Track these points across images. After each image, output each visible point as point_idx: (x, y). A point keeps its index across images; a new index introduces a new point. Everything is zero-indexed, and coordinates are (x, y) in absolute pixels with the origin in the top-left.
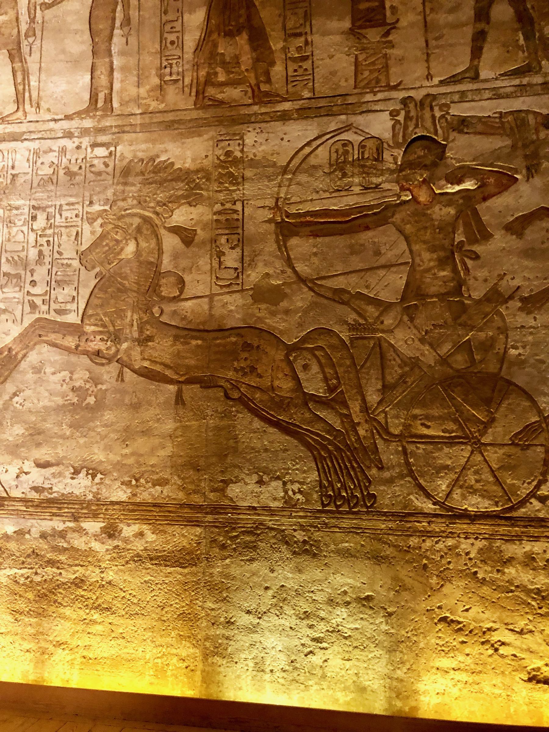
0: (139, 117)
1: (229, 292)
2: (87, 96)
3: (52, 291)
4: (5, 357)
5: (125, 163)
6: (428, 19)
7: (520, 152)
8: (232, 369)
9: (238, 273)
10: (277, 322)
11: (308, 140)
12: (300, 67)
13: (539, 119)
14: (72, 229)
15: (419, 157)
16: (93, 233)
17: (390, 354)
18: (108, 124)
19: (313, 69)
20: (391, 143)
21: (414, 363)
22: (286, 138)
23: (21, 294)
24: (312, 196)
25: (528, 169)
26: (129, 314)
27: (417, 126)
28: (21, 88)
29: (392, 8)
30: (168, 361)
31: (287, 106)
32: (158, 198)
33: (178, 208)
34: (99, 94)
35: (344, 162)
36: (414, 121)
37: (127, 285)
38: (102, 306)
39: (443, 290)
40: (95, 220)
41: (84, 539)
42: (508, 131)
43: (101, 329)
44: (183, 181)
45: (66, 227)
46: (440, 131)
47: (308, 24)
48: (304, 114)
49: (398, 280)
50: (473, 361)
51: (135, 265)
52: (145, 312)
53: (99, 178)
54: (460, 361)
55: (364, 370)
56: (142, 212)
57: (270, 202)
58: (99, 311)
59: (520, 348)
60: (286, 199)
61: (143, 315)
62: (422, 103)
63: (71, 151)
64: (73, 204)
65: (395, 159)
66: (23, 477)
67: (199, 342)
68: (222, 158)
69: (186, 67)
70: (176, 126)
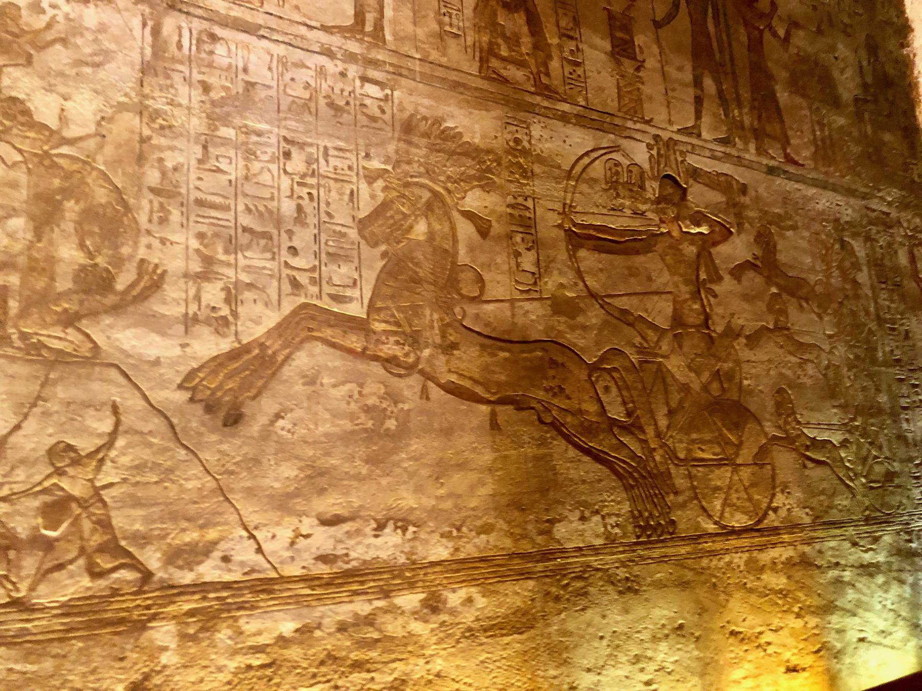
0: (417, 62)
1: (528, 300)
3: (323, 268)
4: (255, 357)
5: (406, 115)
14: (345, 185)
16: (373, 197)
18: (380, 57)
23: (276, 263)
26: (428, 312)
30: (477, 376)
31: (566, 107)
37: (422, 275)
38: (392, 297)
41: (400, 621)
43: (394, 328)
44: (473, 159)
45: (336, 180)
53: (374, 125)
56: (431, 184)
57: (558, 206)
58: (390, 303)
61: (444, 316)
64: (341, 150)
66: (302, 543)
67: (507, 355)
70: (462, 89)
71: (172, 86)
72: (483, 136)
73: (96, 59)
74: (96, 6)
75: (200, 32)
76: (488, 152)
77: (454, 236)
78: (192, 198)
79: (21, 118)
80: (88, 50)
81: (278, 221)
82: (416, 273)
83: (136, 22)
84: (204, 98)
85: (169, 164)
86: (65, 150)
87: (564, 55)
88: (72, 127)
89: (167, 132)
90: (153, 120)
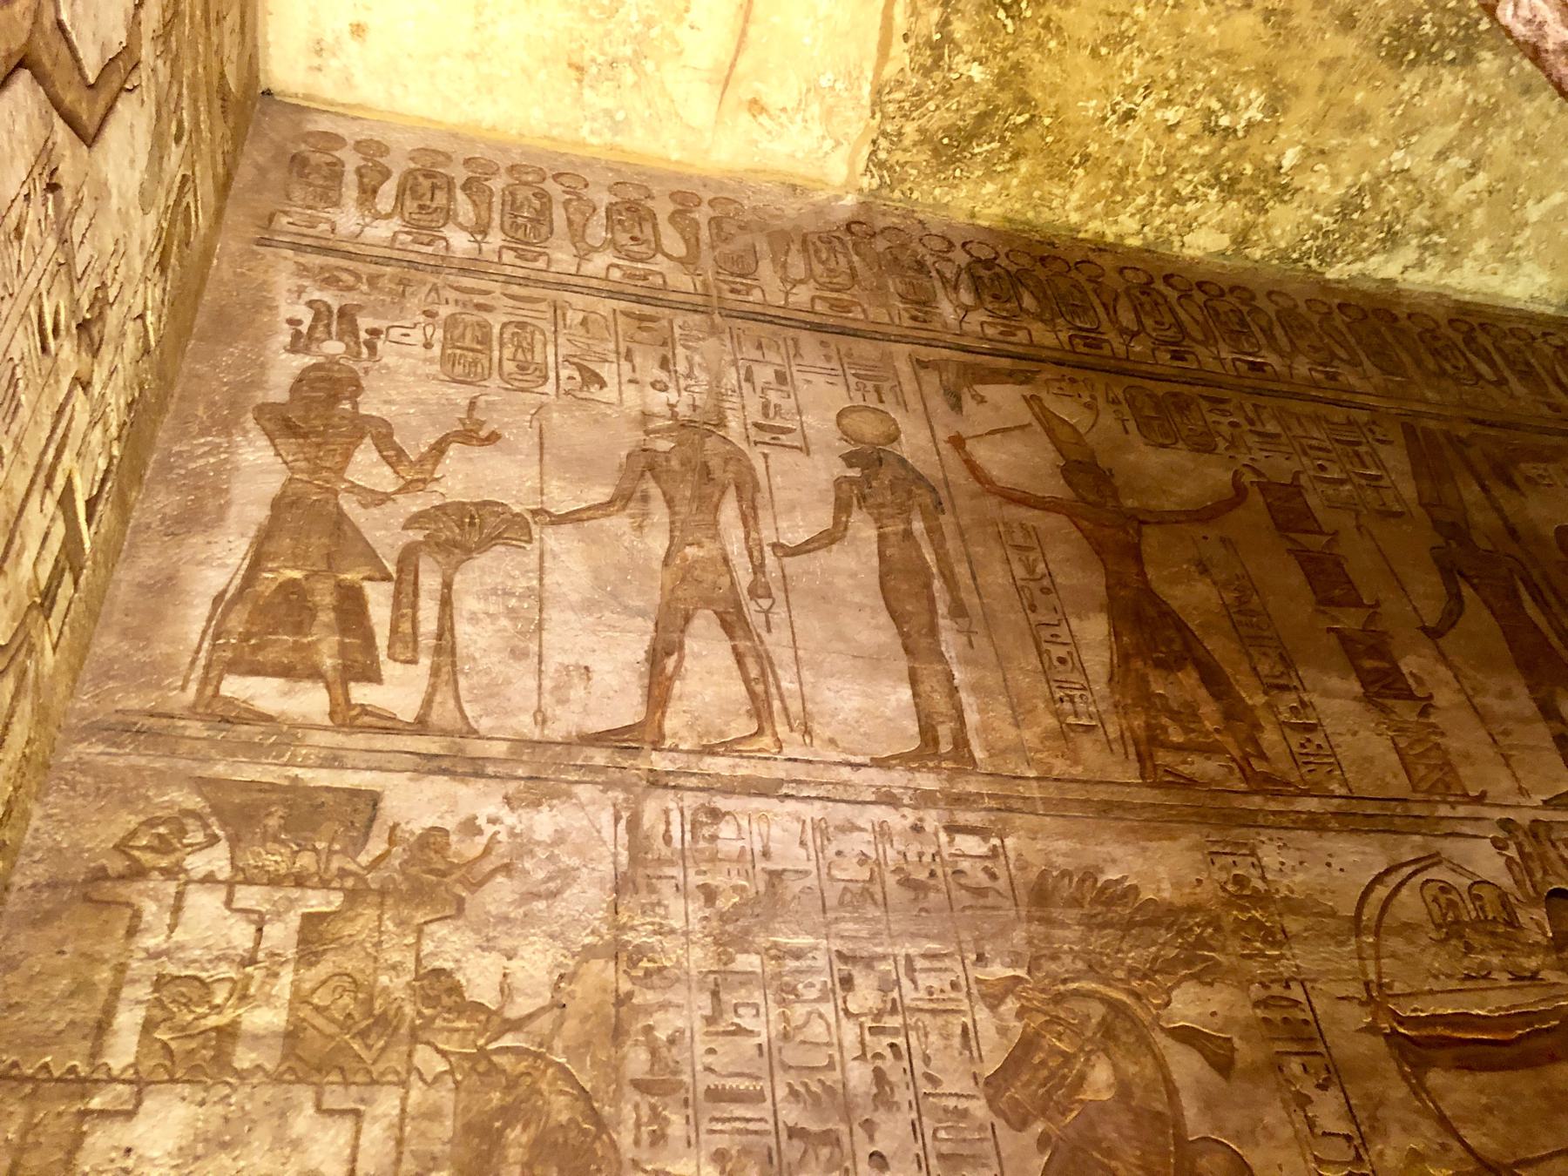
0: (1034, 784)
5: (1033, 874)
12: (1309, 740)
14: (951, 1018)
16: (1003, 1031)
18: (972, 788)
28: (759, 688)
31: (1311, 804)
33: (1178, 984)
34: (939, 728)
40: (1001, 1000)
44: (1168, 929)
45: (933, 1012)
51: (1125, 1118)
53: (981, 902)
56: (1101, 988)
57: (1355, 989)
63: (900, 834)
69: (1102, 707)
70: (1118, 813)
71: (659, 904)
72: (1177, 885)
73: (552, 885)
74: (551, 808)
75: (695, 813)
76: (1191, 910)
77: (1168, 1080)
78: (701, 1088)
79: (446, 1000)
80: (541, 875)
81: (847, 1110)
83: (606, 818)
84: (708, 912)
85: (662, 1035)
86: (508, 1040)
87: (1282, 718)
88: (519, 1000)
89: (656, 979)
90: (634, 964)
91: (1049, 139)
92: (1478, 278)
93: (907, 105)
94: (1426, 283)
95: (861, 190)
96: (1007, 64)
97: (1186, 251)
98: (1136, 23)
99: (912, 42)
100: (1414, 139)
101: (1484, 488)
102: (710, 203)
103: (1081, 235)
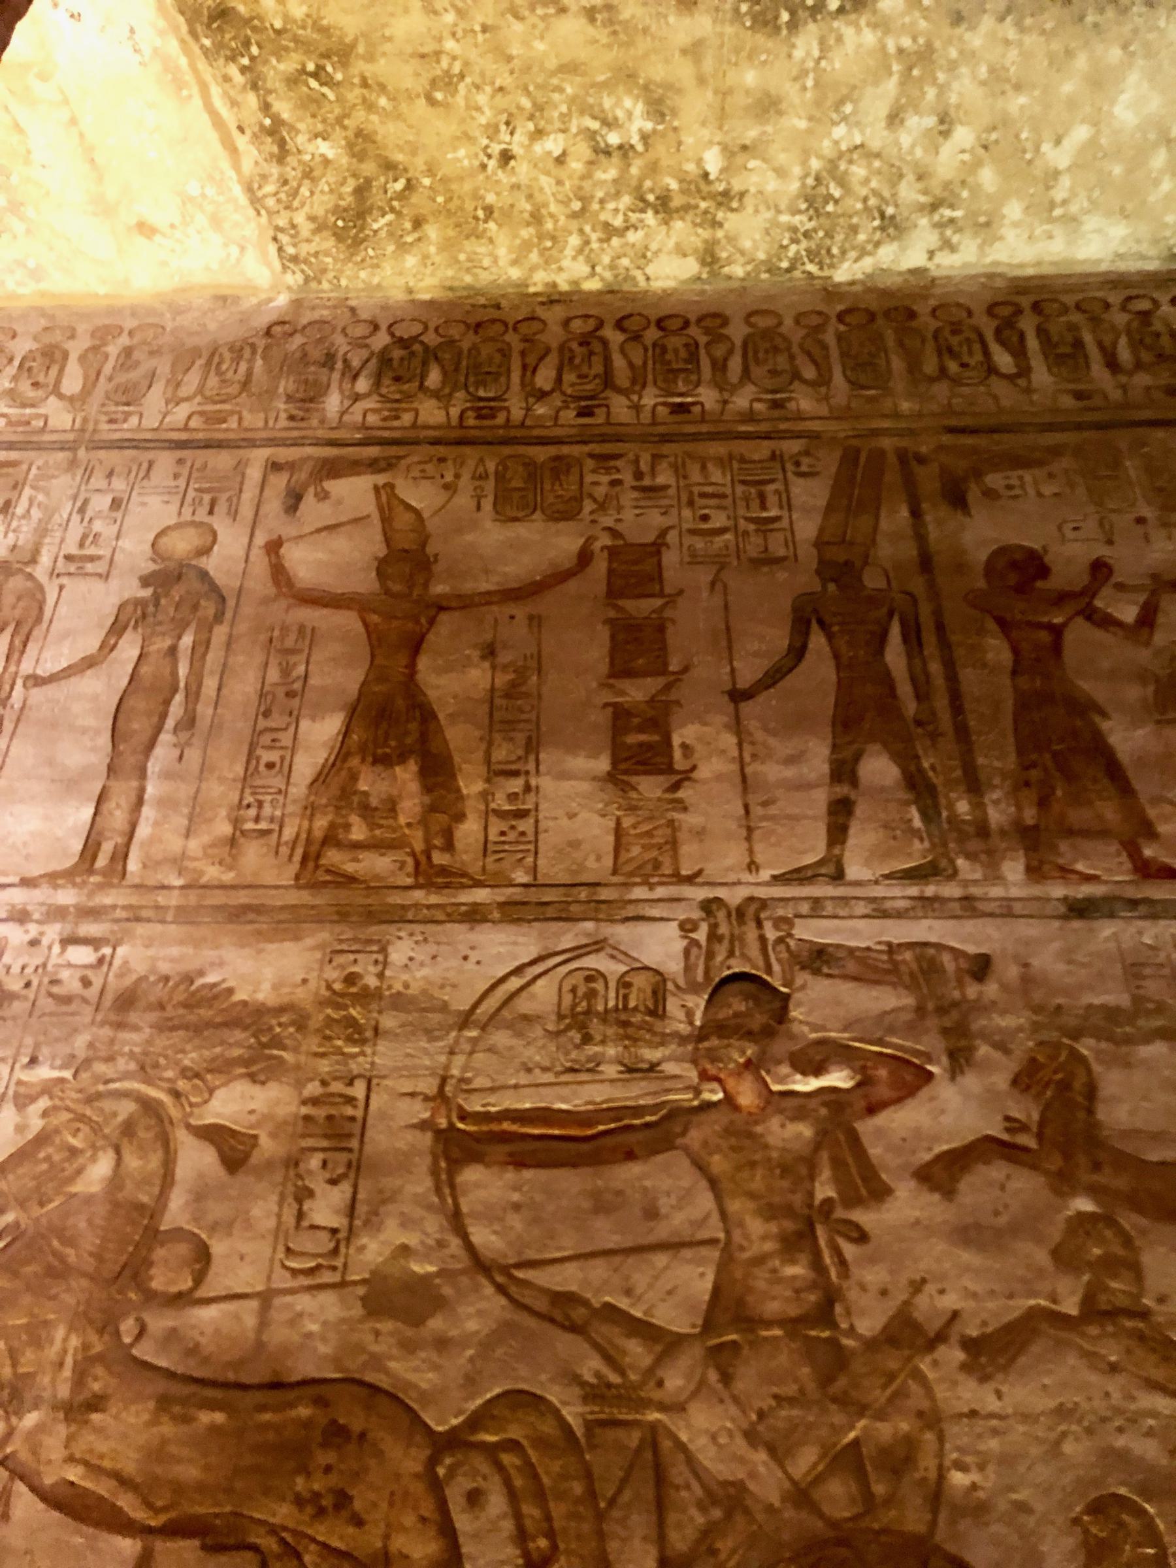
0: (176, 892)
1: (310, 1289)
2: (77, 846)
5: (128, 981)
6: (749, 770)
7: (932, 1022)
8: (290, 1496)
9: (338, 1242)
10: (416, 1370)
11: (517, 964)
12: (513, 827)
13: (964, 964)
15: (737, 1015)
17: (678, 1473)
18: (108, 900)
19: (536, 833)
20: (681, 982)
21: (731, 1498)
22: (474, 956)
24: (519, 1079)
25: (952, 1055)
26: (60, 1333)
27: (731, 954)
29: (685, 747)
32: (187, 1062)
35: (588, 1012)
36: (726, 942)
39: (793, 1311)
40: (33, 1099)
42: (907, 979)
46: (776, 968)
47: (532, 758)
48: (514, 913)
49: (696, 1279)
50: (868, 1496)
51: (101, 1210)
52: (101, 1331)
53: (64, 1008)
54: (838, 1497)
55: (616, 1513)
57: (428, 1086)
59: (974, 1469)
60: (462, 1080)
61: (93, 1338)
62: (740, 913)
65: (690, 1014)
68: (337, 986)
70: (251, 916)
82: (62, 1259)
91: (440, 199)
92: (1022, 247)
93: (283, 196)
94: (965, 265)
95: (289, 288)
96: (350, 134)
97: (658, 285)
98: (454, 58)
99: (248, 132)
100: (848, 108)
101: (916, 513)
102: (131, 333)
103: (532, 290)
